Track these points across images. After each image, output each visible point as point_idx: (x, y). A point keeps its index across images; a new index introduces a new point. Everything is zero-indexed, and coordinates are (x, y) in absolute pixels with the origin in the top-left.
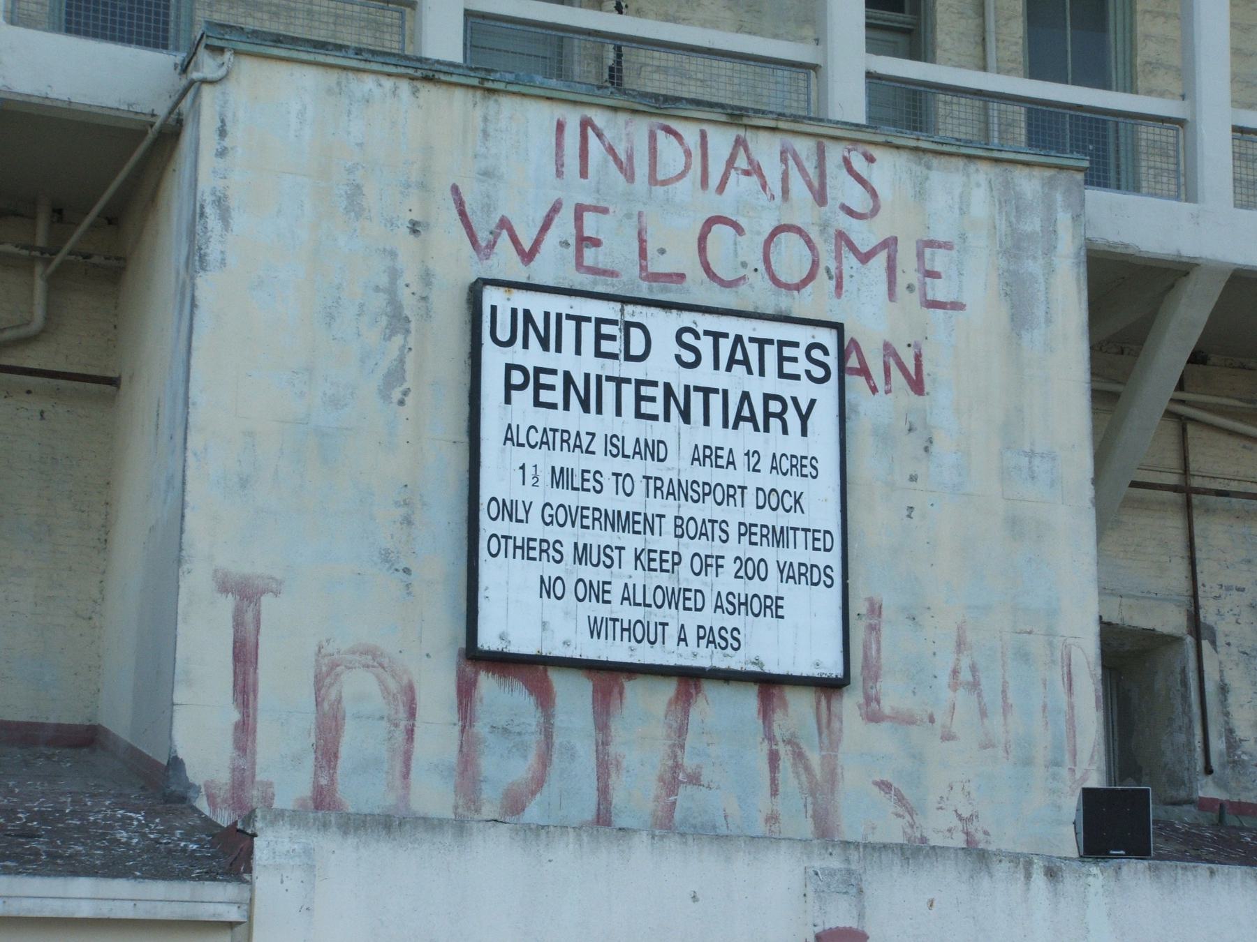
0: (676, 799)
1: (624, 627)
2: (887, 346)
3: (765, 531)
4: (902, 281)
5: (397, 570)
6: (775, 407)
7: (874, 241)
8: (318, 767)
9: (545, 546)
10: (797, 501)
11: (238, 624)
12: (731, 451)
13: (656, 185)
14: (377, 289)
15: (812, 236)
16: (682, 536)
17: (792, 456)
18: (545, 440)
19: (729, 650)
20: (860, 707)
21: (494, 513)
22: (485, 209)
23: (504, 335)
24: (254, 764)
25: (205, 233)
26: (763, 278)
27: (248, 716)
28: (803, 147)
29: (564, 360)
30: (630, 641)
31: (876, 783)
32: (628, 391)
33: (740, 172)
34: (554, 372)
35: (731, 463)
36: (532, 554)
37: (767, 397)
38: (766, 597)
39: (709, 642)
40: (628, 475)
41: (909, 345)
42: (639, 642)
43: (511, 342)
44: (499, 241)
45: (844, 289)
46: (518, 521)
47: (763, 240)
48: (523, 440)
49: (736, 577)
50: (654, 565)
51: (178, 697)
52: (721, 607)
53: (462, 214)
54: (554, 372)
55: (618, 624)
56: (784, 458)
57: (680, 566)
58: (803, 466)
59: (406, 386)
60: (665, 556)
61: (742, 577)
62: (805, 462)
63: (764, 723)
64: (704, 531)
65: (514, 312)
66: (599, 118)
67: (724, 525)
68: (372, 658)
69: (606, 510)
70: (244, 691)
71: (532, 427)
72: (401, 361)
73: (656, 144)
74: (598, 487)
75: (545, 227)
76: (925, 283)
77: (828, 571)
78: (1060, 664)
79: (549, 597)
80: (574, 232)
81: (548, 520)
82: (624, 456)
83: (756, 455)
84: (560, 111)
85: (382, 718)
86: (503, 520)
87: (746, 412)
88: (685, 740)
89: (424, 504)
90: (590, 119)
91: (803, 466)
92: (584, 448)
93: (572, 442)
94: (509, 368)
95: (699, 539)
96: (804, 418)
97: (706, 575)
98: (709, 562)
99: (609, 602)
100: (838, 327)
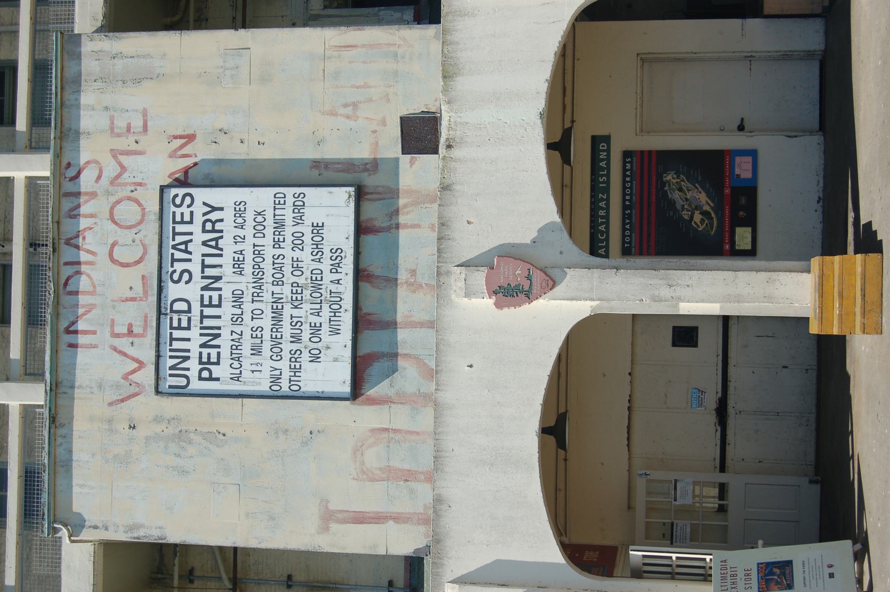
0: (425, 283)
1: (333, 315)
2: (171, 156)
3: (277, 233)
4: (134, 147)
6: (209, 226)
7: (114, 163)
8: (416, 480)
9: (293, 360)
10: (259, 214)
11: (344, 521)
12: (235, 252)
13: (96, 291)
14: (166, 447)
15: (115, 200)
16: (283, 281)
17: (235, 216)
18: (237, 359)
19: (342, 255)
20: (370, 175)
22: (119, 387)
24: (415, 513)
25: (147, 537)
27: (391, 516)
29: (194, 347)
30: (340, 312)
31: (411, 166)
32: (208, 311)
33: (84, 243)
34: (201, 353)
35: (241, 252)
36: (298, 367)
37: (204, 231)
38: (313, 233)
39: (339, 267)
40: (252, 312)
44: (135, 380)
46: (281, 375)
47: (119, 229)
48: (238, 371)
49: (303, 250)
50: (299, 298)
51: (383, 552)
52: (320, 259)
53: (122, 401)
54: (201, 353)
55: (332, 319)
56: (236, 221)
57: (299, 283)
58: (240, 211)
60: (294, 292)
61: (303, 247)
62: (237, 209)
64: (279, 269)
67: (276, 257)
68: (358, 450)
70: (378, 519)
72: (202, 434)
73: (74, 291)
74: (260, 329)
75: (125, 355)
77: (296, 196)
78: (340, 52)
79: (320, 357)
80: (125, 338)
81: (279, 358)
82: (242, 314)
83: (236, 238)
85: (388, 446)
86: (281, 383)
87: (213, 243)
88: (392, 278)
89: (276, 422)
90: (65, 328)
92: (241, 337)
94: (200, 378)
95: (283, 271)
96: (214, 209)
97: (303, 268)
98: (296, 266)
99: (321, 323)
100: (162, 189)
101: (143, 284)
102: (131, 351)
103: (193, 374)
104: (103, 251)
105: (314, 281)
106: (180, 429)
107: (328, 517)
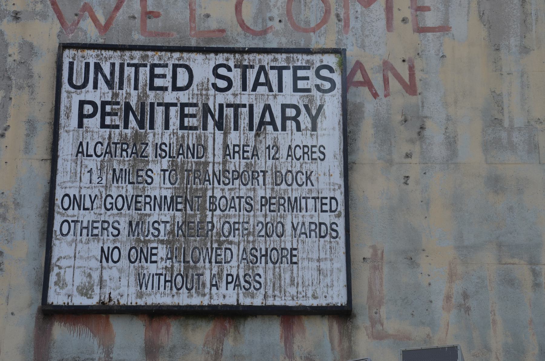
4: (397, 16)
6: (291, 112)
9: (106, 225)
10: (308, 178)
16: (215, 210)
17: (304, 146)
21: (66, 205)
23: (78, 80)
26: (285, 25)
36: (95, 232)
37: (284, 107)
41: (404, 61)
43: (84, 85)
45: (351, 27)
48: (91, 152)
55: (162, 278)
56: (298, 148)
61: (263, 236)
62: (314, 149)
63: (285, 345)
64: (233, 205)
65: (87, 65)
69: (155, 197)
74: (149, 180)
76: (417, 16)
77: (334, 226)
81: (109, 206)
83: (275, 148)
87: (268, 118)
93: (129, 151)
99: (156, 262)
103: (89, 94)
105: (216, 252)
106: (13, 77)
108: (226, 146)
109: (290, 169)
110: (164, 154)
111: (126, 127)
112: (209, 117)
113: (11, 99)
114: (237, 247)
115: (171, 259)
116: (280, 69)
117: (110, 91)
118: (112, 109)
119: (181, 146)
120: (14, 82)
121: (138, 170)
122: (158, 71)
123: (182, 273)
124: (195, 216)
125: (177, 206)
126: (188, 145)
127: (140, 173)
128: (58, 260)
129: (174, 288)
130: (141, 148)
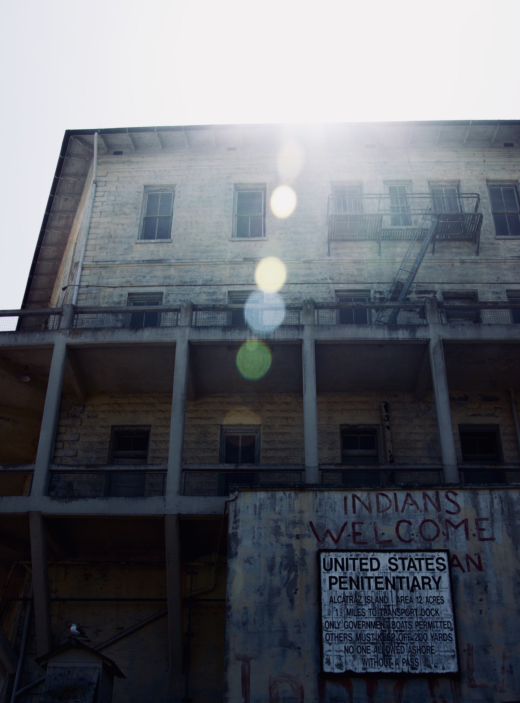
4: (471, 533)
5: (296, 648)
6: (426, 580)
7: (459, 521)
9: (346, 636)
10: (437, 612)
15: (436, 522)
16: (395, 628)
17: (434, 597)
21: (327, 627)
26: (420, 538)
28: (431, 493)
36: (341, 639)
37: (423, 578)
42: (381, 666)
48: (336, 601)
52: (411, 651)
55: (373, 661)
58: (438, 600)
59: (297, 587)
61: (418, 640)
62: (438, 598)
64: (403, 626)
65: (331, 559)
66: (359, 494)
71: (339, 596)
72: (295, 579)
74: (364, 614)
76: (479, 533)
77: (450, 635)
81: (346, 627)
83: (420, 598)
84: (345, 494)
87: (416, 584)
90: (356, 495)
91: (438, 600)
93: (353, 600)
94: (331, 578)
96: (437, 583)
99: (370, 653)
101: (386, 541)
102: (344, 535)
103: (333, 573)
104: (404, 516)
105: (397, 648)
106: (298, 565)
107: (246, 660)
108: (397, 597)
109: (428, 608)
110: (369, 601)
111: (351, 588)
112: (389, 583)
113: (298, 575)
114: (406, 646)
115: (376, 651)
116: (420, 560)
117: (343, 572)
118: (344, 580)
119: (377, 597)
120: (298, 567)
121: (358, 609)
122: (363, 561)
123: (382, 658)
124: (386, 631)
125: (377, 627)
126: (380, 597)
127: (359, 611)
128: (326, 652)
129: (379, 665)
130: (359, 598)
